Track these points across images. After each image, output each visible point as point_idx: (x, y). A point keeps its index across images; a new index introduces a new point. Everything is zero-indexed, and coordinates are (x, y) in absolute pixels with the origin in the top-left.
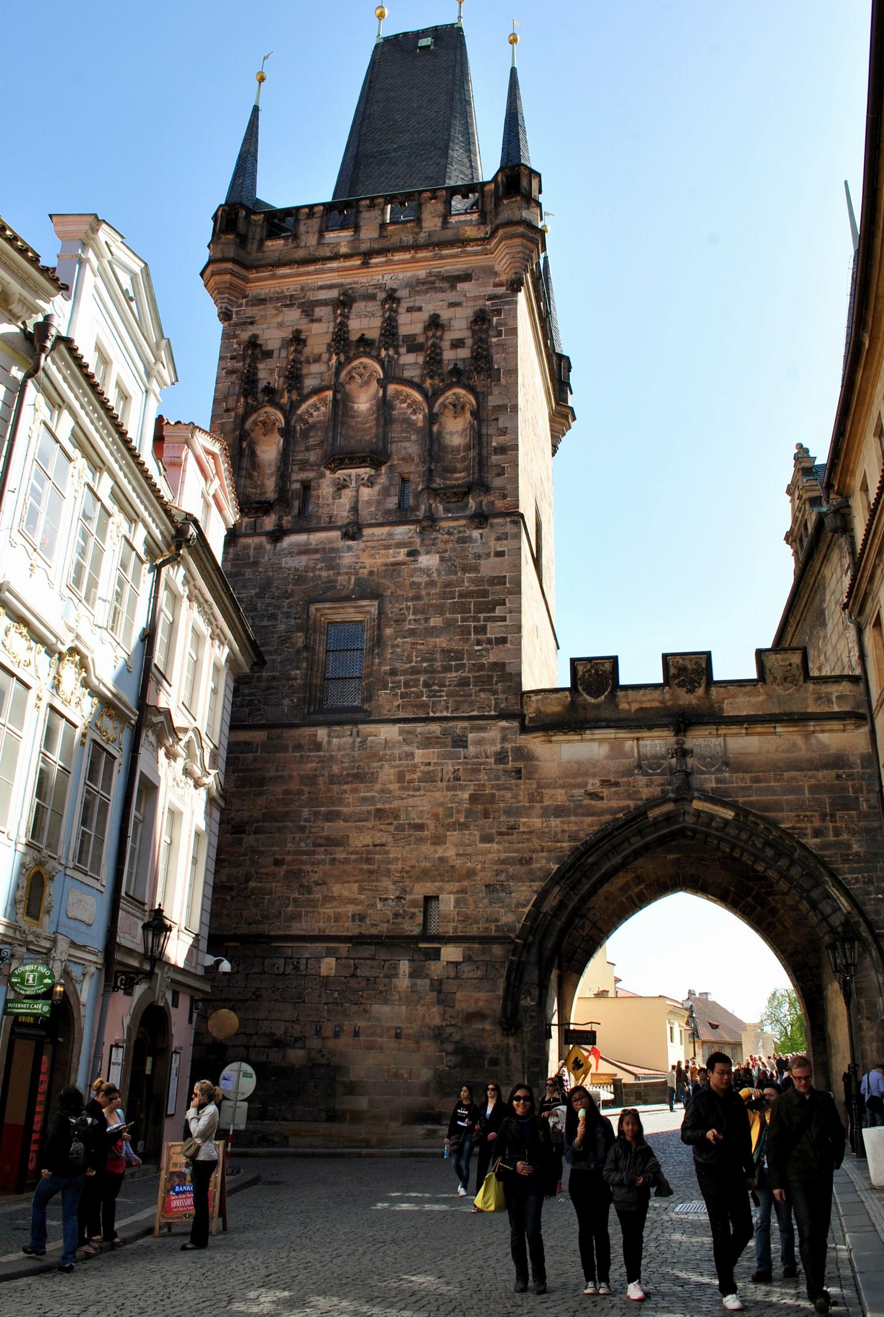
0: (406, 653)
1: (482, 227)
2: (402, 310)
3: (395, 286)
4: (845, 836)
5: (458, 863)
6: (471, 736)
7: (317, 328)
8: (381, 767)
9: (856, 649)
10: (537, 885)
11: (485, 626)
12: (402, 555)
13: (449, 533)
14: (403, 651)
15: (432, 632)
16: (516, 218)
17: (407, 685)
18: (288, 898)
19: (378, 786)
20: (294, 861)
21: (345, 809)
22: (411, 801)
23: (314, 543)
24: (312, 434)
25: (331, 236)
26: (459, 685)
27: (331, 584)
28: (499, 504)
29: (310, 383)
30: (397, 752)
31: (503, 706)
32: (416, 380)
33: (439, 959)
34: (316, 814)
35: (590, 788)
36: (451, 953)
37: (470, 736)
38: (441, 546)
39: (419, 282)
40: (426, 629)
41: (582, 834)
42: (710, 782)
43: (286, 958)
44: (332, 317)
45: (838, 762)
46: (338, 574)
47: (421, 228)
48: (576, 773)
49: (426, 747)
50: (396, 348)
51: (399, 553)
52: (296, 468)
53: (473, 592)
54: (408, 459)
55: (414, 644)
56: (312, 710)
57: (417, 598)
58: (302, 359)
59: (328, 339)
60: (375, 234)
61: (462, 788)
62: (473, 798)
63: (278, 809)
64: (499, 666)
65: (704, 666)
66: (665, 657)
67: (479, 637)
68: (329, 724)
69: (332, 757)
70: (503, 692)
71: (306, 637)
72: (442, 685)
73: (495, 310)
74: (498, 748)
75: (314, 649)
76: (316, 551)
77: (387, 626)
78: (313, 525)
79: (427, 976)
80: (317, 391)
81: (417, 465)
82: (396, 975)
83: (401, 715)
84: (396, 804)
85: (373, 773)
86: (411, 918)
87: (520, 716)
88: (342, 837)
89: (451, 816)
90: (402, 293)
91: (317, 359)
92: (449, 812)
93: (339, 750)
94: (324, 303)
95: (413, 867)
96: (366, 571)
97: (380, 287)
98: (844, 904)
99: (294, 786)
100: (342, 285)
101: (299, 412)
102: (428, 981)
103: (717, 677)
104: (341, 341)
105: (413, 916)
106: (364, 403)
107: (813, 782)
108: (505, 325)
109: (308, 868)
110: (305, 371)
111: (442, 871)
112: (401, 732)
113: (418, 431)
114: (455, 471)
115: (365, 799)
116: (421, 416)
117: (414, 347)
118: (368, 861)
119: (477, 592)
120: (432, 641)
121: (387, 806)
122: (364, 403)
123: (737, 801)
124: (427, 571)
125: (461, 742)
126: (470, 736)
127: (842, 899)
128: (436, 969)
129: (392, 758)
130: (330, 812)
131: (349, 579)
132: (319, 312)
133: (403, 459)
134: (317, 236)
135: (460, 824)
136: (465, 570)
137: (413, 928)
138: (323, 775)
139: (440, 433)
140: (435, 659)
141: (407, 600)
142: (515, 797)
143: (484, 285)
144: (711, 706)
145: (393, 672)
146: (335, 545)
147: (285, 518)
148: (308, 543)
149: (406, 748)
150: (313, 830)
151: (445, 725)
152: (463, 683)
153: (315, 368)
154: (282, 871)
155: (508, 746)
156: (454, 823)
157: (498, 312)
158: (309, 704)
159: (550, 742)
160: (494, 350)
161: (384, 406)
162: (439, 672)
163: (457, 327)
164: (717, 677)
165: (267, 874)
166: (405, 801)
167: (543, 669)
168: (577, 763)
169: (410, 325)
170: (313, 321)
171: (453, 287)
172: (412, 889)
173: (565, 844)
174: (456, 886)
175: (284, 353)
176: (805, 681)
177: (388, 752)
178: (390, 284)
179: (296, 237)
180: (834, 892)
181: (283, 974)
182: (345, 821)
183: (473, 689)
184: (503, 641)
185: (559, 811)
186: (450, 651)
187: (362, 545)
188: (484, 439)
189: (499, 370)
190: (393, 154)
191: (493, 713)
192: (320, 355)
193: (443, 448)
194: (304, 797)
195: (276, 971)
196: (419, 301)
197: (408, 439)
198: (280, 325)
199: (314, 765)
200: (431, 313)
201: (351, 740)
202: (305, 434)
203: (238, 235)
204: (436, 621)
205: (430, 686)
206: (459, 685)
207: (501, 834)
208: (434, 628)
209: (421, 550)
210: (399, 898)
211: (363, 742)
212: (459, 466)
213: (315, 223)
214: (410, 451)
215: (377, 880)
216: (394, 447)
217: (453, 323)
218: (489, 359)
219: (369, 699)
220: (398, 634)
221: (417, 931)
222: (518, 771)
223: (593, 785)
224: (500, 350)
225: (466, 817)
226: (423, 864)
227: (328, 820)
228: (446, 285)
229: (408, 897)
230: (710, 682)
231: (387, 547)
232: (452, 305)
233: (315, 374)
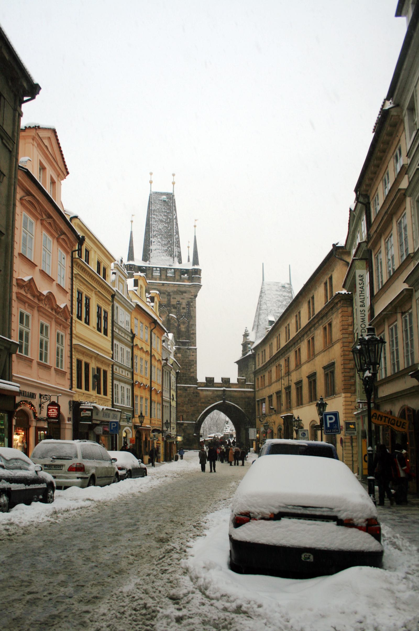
62: (189, 400)
90: (171, 294)
92: (184, 402)
97: (167, 291)
113: (176, 327)
152: (186, 379)
157: (192, 302)
167: (201, 378)
171: (182, 294)
178: (169, 291)
185: (203, 403)
196: (175, 296)
197: (173, 329)
222: (196, 396)
230: (229, 384)
232: (182, 299)
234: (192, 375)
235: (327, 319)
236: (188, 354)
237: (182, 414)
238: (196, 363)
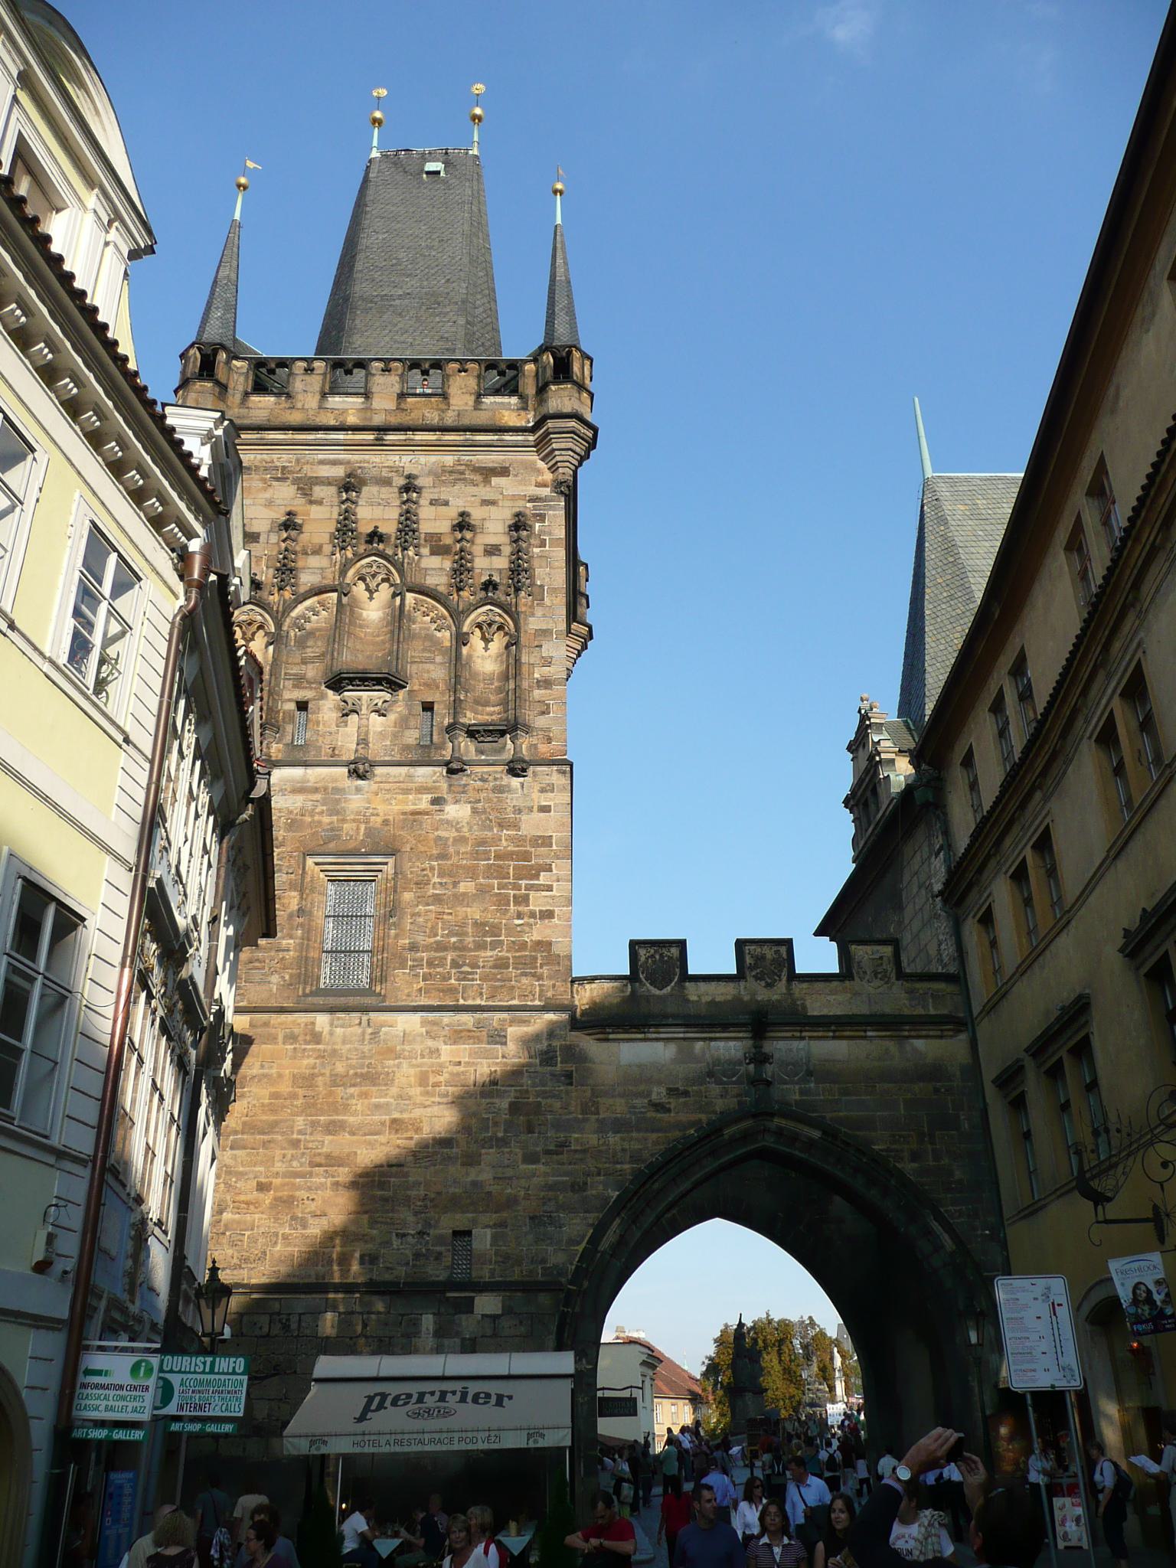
0: (429, 925)
1: (523, 413)
3: (415, 472)
4: (945, 1161)
5: (494, 1189)
7: (316, 511)
8: (398, 1066)
9: (951, 942)
10: (593, 1217)
11: (528, 895)
12: (424, 802)
13: (482, 780)
14: (426, 921)
15: (461, 899)
17: (430, 963)
18: (276, 1234)
19: (394, 1090)
20: (283, 1185)
21: (351, 1119)
23: (312, 779)
24: (309, 644)
25: (335, 401)
26: (495, 967)
27: (334, 833)
28: (544, 749)
29: (307, 579)
30: (418, 1048)
31: (549, 994)
32: (442, 589)
33: (472, 1312)
34: (314, 1124)
35: (654, 1096)
36: (487, 1304)
37: (510, 1030)
38: (472, 795)
39: (445, 470)
40: (455, 895)
41: (646, 1154)
42: (793, 1093)
43: (271, 1315)
44: (336, 501)
45: (934, 1073)
46: (344, 821)
47: (448, 404)
48: (638, 1079)
49: (455, 1043)
51: (420, 799)
52: (289, 684)
53: (512, 853)
54: (431, 685)
55: (440, 913)
56: (308, 991)
57: (443, 856)
58: (298, 548)
59: (332, 527)
60: (392, 406)
62: (514, 1108)
63: (264, 1118)
64: (544, 945)
65: (785, 956)
66: (740, 944)
67: (520, 909)
68: (332, 1010)
69: (334, 1051)
70: (550, 978)
71: (302, 898)
72: (474, 966)
73: (540, 515)
75: (310, 913)
76: (316, 790)
77: (405, 889)
78: (311, 756)
79: (457, 1334)
81: (443, 693)
82: (417, 1334)
84: (417, 1113)
85: (388, 1073)
86: (437, 1259)
88: (348, 1155)
89: (487, 1129)
91: (317, 551)
92: (484, 1125)
93: (344, 1042)
95: (439, 1193)
96: (379, 820)
97: (397, 470)
99: (285, 1088)
100: (349, 462)
101: (294, 614)
102: (457, 1341)
104: (345, 529)
105: (439, 1256)
106: (373, 610)
107: (909, 1096)
108: (550, 534)
109: (302, 1194)
110: (300, 564)
111: (477, 1199)
112: (424, 1023)
113: (443, 651)
114: (487, 704)
115: (378, 1106)
116: (447, 634)
117: (439, 550)
118: (382, 1185)
119: (517, 853)
120: (462, 910)
121: (405, 1116)
122: (373, 610)
123: (824, 1118)
126: (510, 1030)
127: (946, 1236)
128: (468, 1325)
130: (333, 1122)
131: (358, 829)
132: (319, 491)
133: (427, 685)
134: (318, 397)
135: (498, 1140)
137: (437, 1272)
138: (323, 1075)
139: (470, 656)
140: (466, 934)
141: (431, 858)
142: (565, 1107)
144: (794, 1002)
145: (413, 947)
146: (339, 785)
147: (274, 745)
148: (305, 780)
149: (430, 1043)
150: (310, 1145)
151: (478, 1015)
152: (501, 964)
153: (314, 561)
154: (267, 1198)
155: (556, 1043)
156: (491, 1139)
157: (542, 518)
158: (305, 983)
159: (607, 1040)
160: (536, 563)
161: (398, 618)
162: (470, 950)
163: (491, 530)
165: (248, 1203)
166: (429, 1110)
168: (639, 1066)
169: (434, 521)
170: (311, 502)
171: (487, 481)
172: (438, 1221)
173: (626, 1166)
175: (274, 538)
176: (898, 979)
177: (407, 1048)
179: (289, 396)
180: (936, 1226)
181: (268, 1335)
182: (352, 1133)
184: (548, 915)
185: (620, 1126)
186: (484, 924)
187: (374, 787)
188: (525, 669)
189: (542, 586)
190: (397, 302)
191: (537, 1003)
192: (321, 546)
193: (474, 675)
194: (299, 1102)
195: (258, 1332)
196: (444, 493)
198: (269, 504)
199: (312, 1061)
200: (461, 510)
201: (359, 1030)
202: (301, 643)
203: (218, 383)
204: (466, 887)
205: (461, 966)
206: (495, 967)
207: (548, 1152)
208: (464, 894)
210: (421, 1233)
211: (375, 1034)
212: (493, 698)
213: (315, 382)
214: (434, 675)
215: (393, 1211)
216: (412, 669)
217: (487, 524)
219: (383, 979)
220: (421, 899)
221: (443, 1276)
222: (569, 1076)
223: (659, 1094)
224: (544, 564)
225: (505, 1131)
226: (452, 1190)
227: (330, 1133)
228: (478, 478)
229: (432, 1232)
232: (486, 503)
233: (312, 571)
236: (513, 800)
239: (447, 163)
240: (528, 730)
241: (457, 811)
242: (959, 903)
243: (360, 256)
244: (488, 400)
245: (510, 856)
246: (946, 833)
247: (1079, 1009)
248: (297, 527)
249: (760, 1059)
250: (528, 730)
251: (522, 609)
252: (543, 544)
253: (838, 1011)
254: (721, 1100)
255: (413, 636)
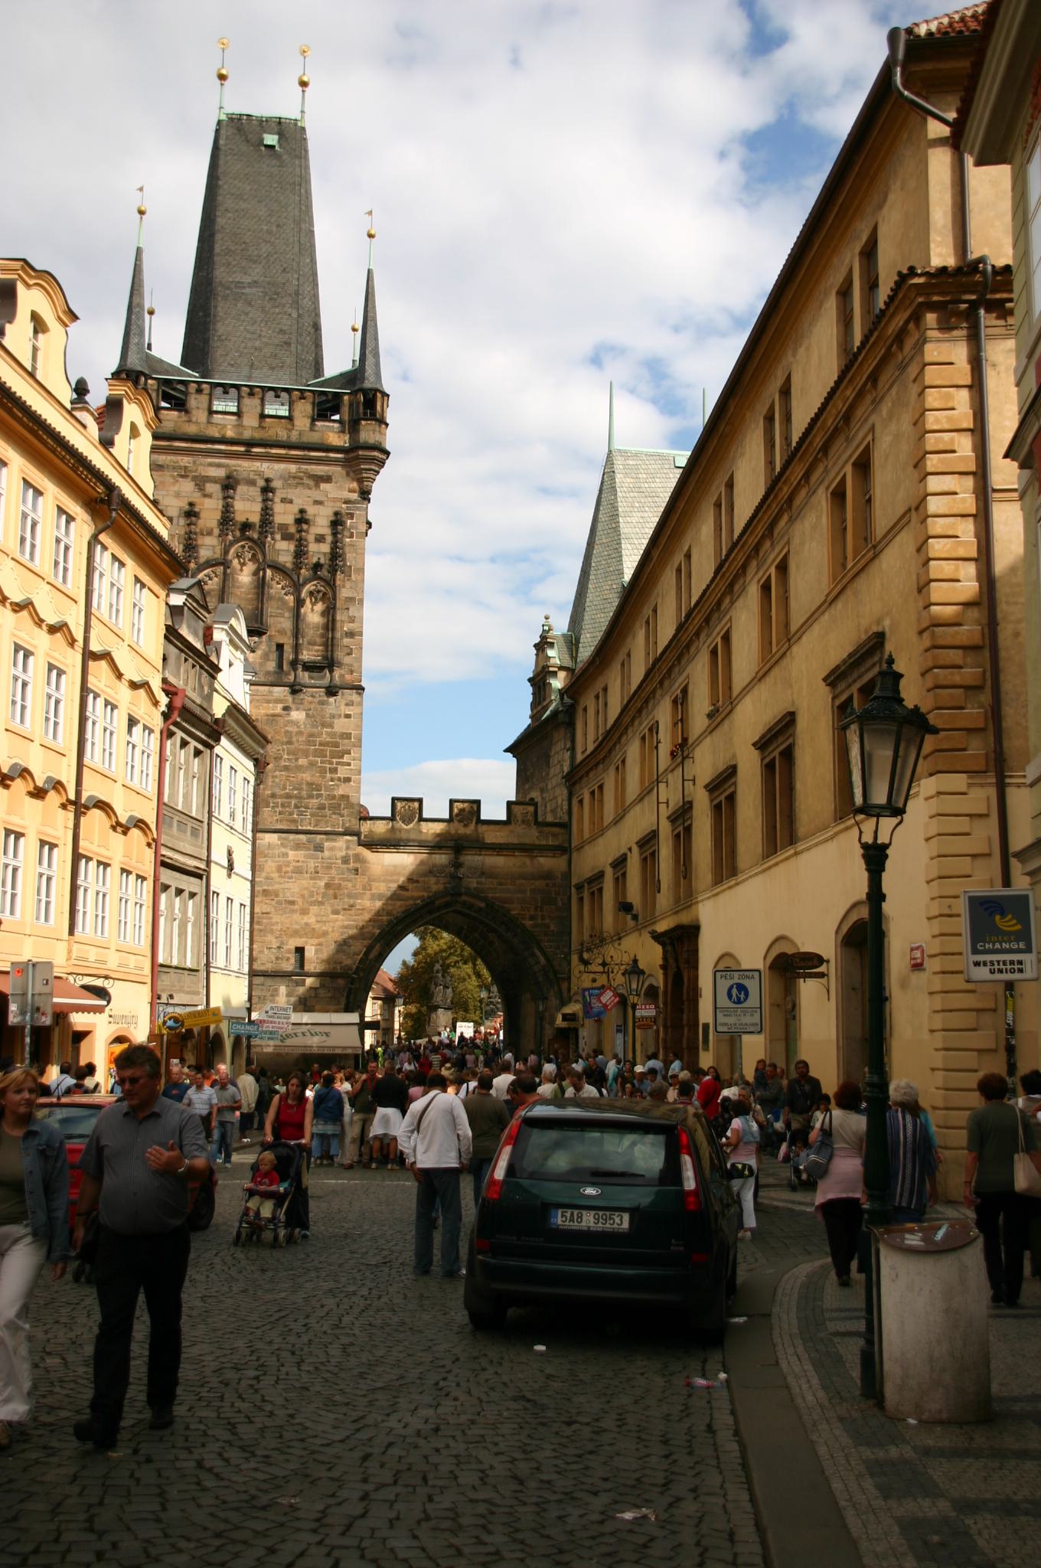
2: (277, 500)
5: (317, 926)
6: (326, 844)
10: (366, 942)
15: (299, 768)
16: (371, 441)
19: (264, 874)
22: (286, 886)
28: (348, 677)
29: (204, 554)
32: (289, 565)
42: (473, 883)
45: (548, 876)
48: (391, 872)
50: (272, 534)
54: (282, 632)
57: (290, 743)
59: (218, 516)
60: (255, 423)
61: (320, 879)
62: (328, 886)
64: (345, 797)
72: (307, 807)
74: (343, 853)
80: (210, 564)
83: (279, 827)
84: (277, 887)
87: (357, 834)
91: (210, 533)
94: (214, 480)
97: (259, 473)
98: (542, 960)
103: (483, 817)
104: (226, 518)
105: (288, 959)
110: (200, 542)
111: (308, 931)
114: (314, 644)
117: (287, 537)
124: (295, 723)
125: (319, 848)
129: (273, 856)
132: (211, 488)
136: (323, 725)
137: (289, 965)
143: (340, 488)
145: (273, 796)
152: (322, 807)
155: (351, 853)
160: (347, 549)
164: (483, 817)
168: (395, 866)
169: (284, 515)
170: (205, 496)
171: (317, 486)
174: (315, 941)
178: (268, 474)
179: (187, 412)
183: (327, 812)
184: (348, 780)
188: (338, 625)
190: (247, 291)
196: (291, 493)
198: (178, 495)
204: (302, 761)
209: (293, 706)
216: (270, 621)
218: (342, 556)
228: (311, 483)
231: (268, 702)
232: (318, 503)
234: (341, 790)
235: (848, 440)
237: (299, 942)
238: (359, 744)
239: (281, 135)
240: (340, 665)
241: (297, 715)
242: (574, 784)
243: (218, 236)
244: (319, 424)
245: (326, 744)
246: (573, 741)
247: (600, 875)
248: (196, 515)
249: (457, 865)
250: (340, 665)
251: (338, 583)
252: (351, 536)
253: (501, 841)
254: (435, 885)
255: (271, 598)
